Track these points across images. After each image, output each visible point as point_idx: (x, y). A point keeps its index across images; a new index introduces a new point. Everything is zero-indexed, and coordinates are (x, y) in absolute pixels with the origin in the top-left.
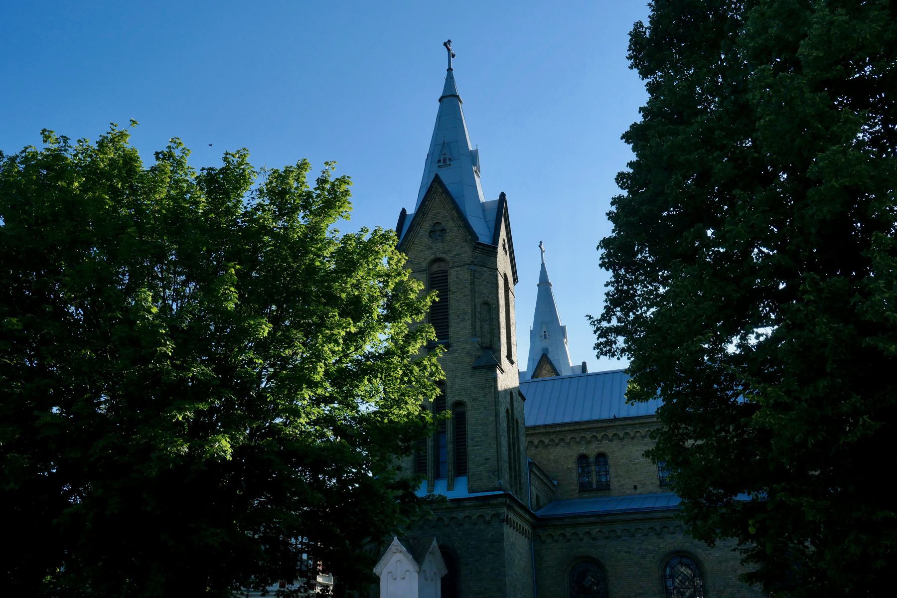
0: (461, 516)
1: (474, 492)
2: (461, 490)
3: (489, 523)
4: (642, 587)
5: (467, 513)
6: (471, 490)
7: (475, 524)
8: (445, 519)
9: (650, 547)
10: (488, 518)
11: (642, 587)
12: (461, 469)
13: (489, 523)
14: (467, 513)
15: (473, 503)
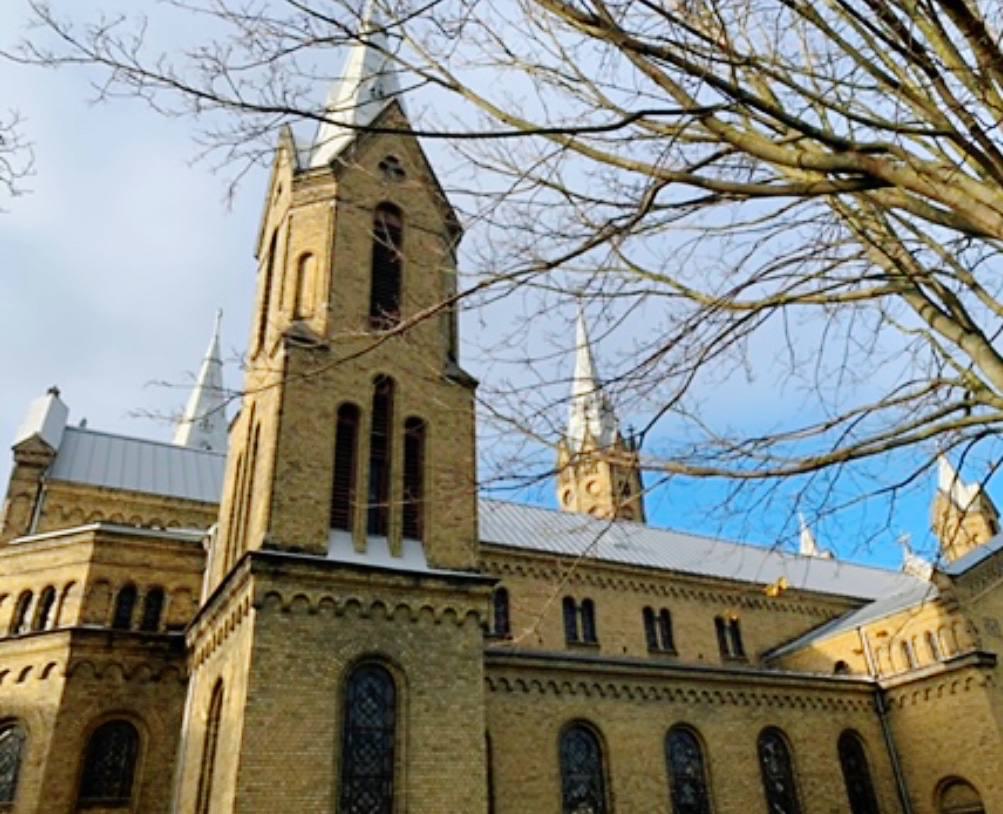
0: (416, 603)
1: (437, 567)
2: (414, 559)
3: (460, 625)
4: (534, 768)
5: (427, 601)
6: (432, 563)
7: (438, 622)
8: (388, 605)
9: (547, 710)
10: (461, 616)
11: (534, 768)
12: (412, 529)
13: (460, 625)
14: (427, 601)
15: (440, 585)
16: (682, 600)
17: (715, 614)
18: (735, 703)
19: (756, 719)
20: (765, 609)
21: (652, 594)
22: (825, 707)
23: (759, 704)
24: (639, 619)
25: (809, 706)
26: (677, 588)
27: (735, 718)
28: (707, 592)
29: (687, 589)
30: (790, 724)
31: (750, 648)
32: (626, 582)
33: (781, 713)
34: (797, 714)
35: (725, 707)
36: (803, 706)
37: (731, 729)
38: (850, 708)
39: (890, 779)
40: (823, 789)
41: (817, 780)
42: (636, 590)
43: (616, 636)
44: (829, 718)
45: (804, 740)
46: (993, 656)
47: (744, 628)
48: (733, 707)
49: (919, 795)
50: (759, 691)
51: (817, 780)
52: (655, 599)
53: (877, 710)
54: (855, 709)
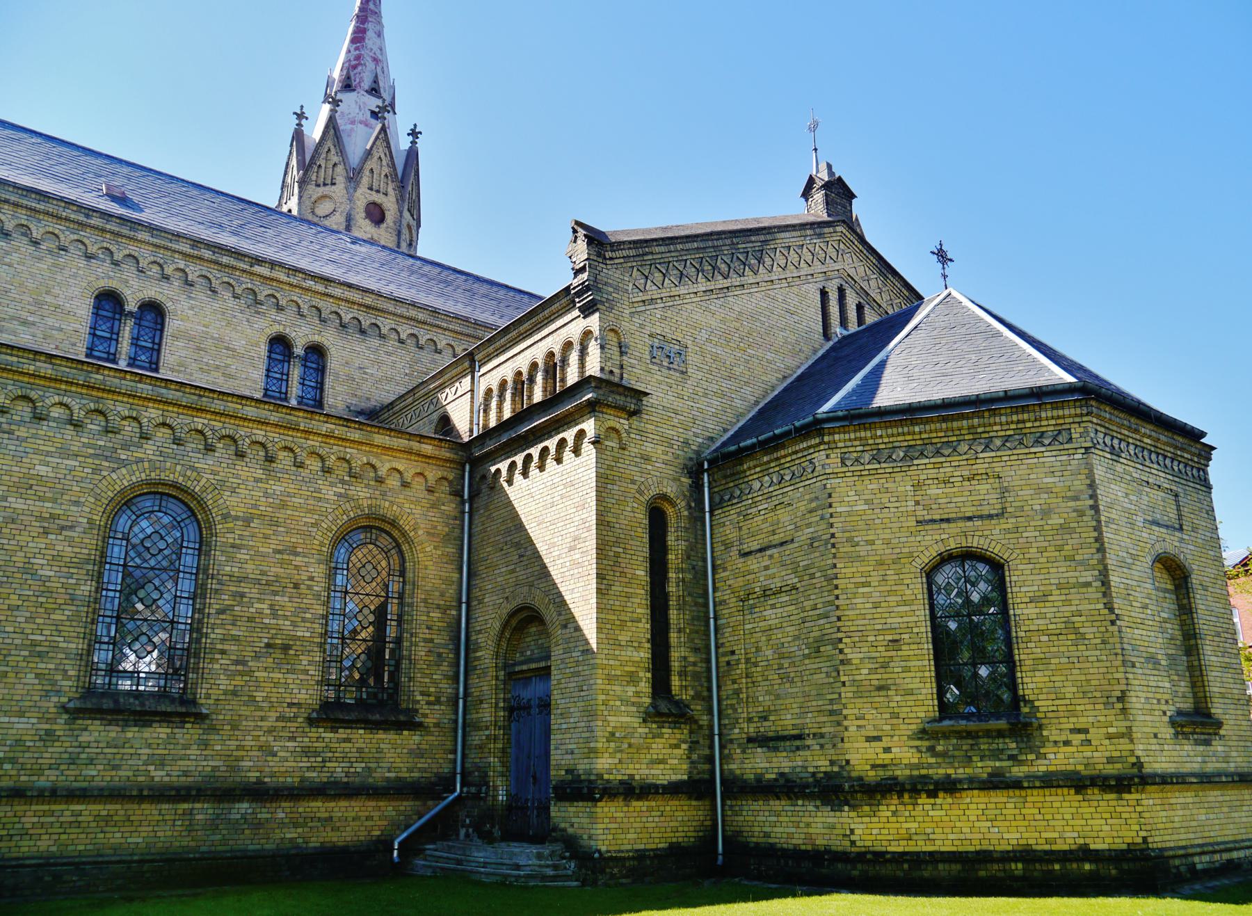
16: (200, 294)
17: (277, 329)
18: (77, 425)
19: (124, 464)
20: (392, 343)
21: (129, 270)
22: (327, 471)
23: (145, 437)
24: (83, 310)
25: (284, 458)
26: (194, 271)
27: (65, 453)
28: (264, 292)
29: (214, 274)
30: (219, 486)
31: (337, 396)
32: (67, 237)
33: (205, 463)
34: (250, 470)
35: (44, 429)
36: (270, 459)
37: (43, 470)
38: (393, 482)
39: (444, 610)
40: (264, 606)
41: (252, 591)
42: (89, 257)
43: (14, 325)
44: (330, 493)
45: (247, 521)
46: (640, 395)
47: (334, 362)
48: (69, 431)
49: (481, 639)
50: (153, 413)
51: (252, 591)
52: (135, 283)
53: (458, 493)
54: (405, 485)
